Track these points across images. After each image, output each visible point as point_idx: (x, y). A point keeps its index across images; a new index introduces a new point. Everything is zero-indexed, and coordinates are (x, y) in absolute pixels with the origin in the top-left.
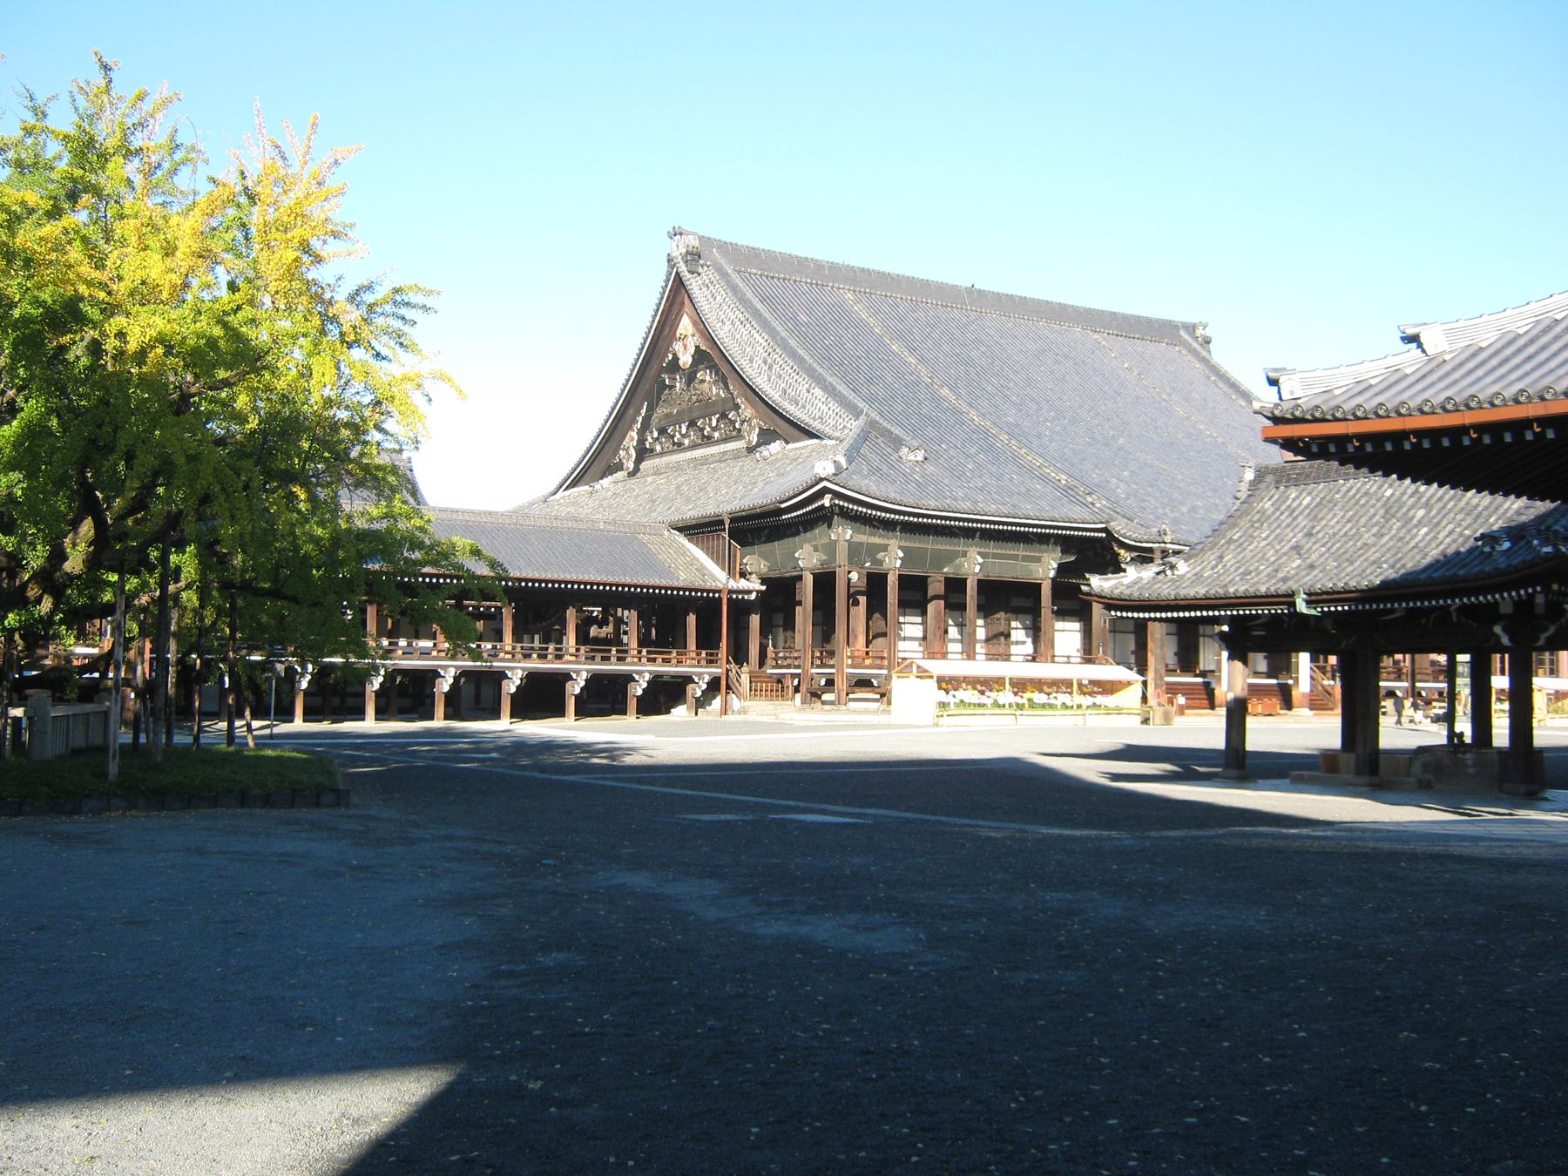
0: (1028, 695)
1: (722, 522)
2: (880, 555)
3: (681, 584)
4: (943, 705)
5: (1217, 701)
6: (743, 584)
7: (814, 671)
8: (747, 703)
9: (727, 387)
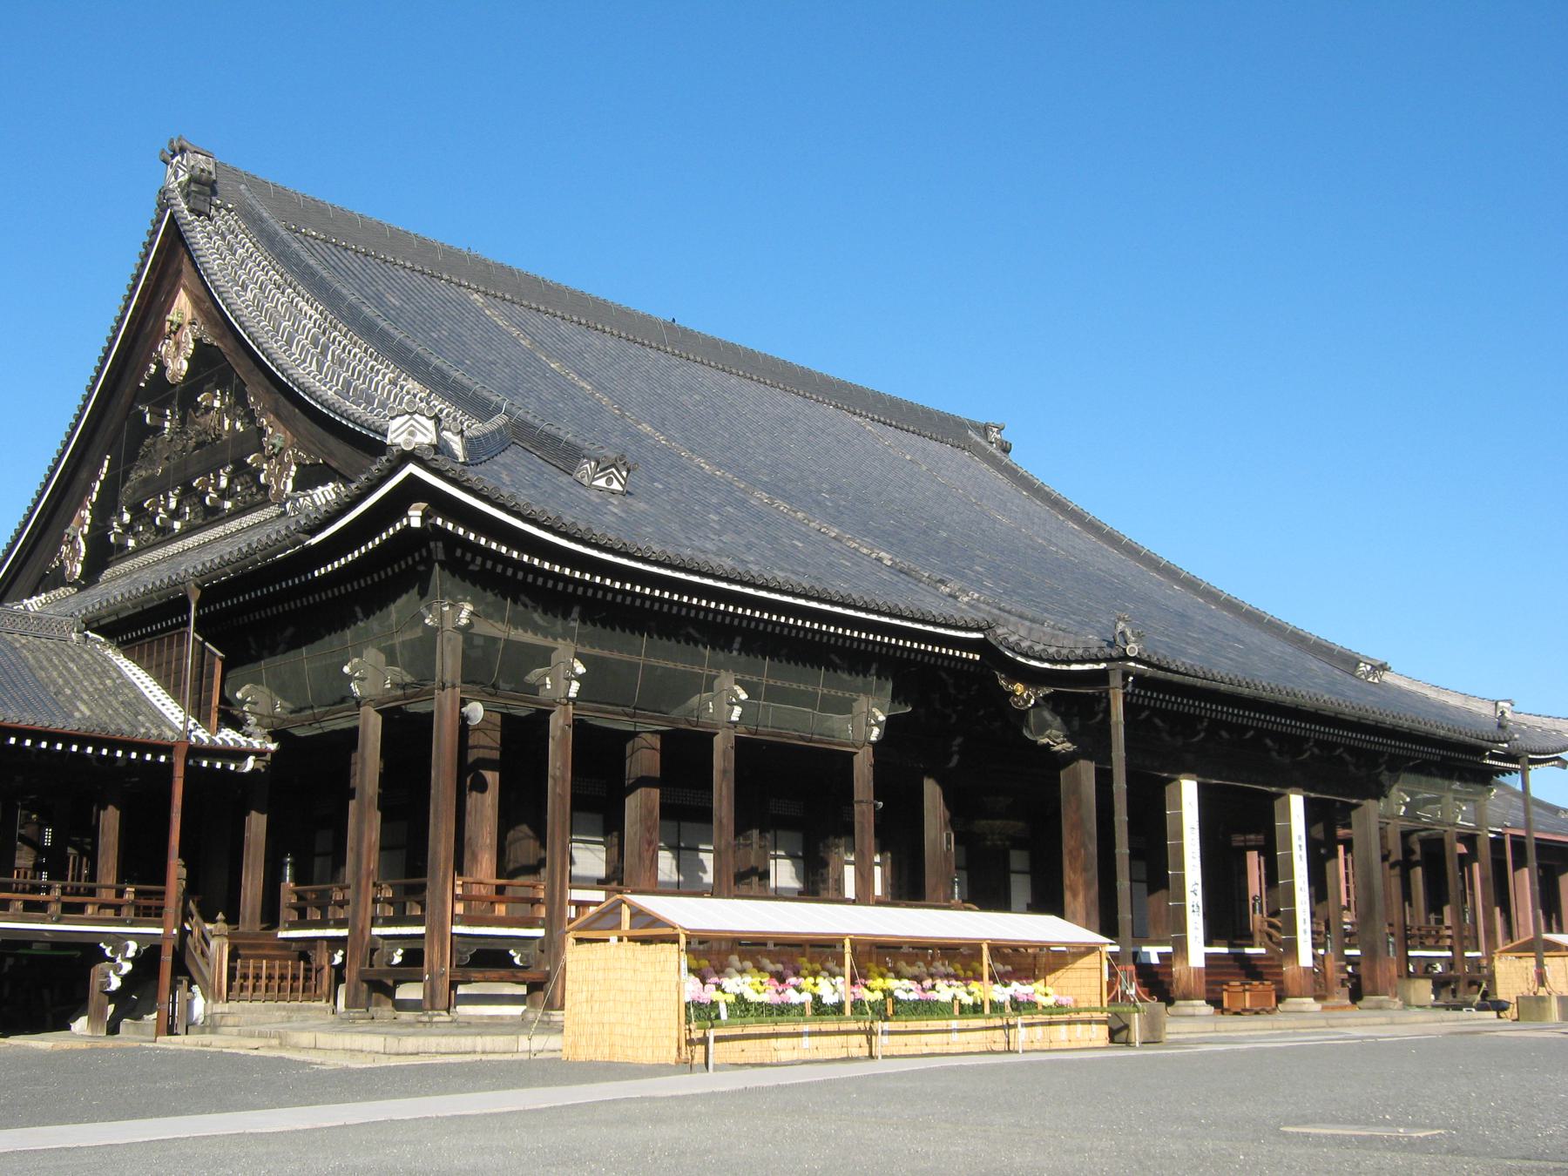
0: (878, 983)
1: (181, 605)
2: (532, 676)
3: (72, 726)
4: (702, 1012)
5: (1177, 990)
6: (228, 736)
7: (376, 931)
8: (221, 1007)
9: (250, 417)
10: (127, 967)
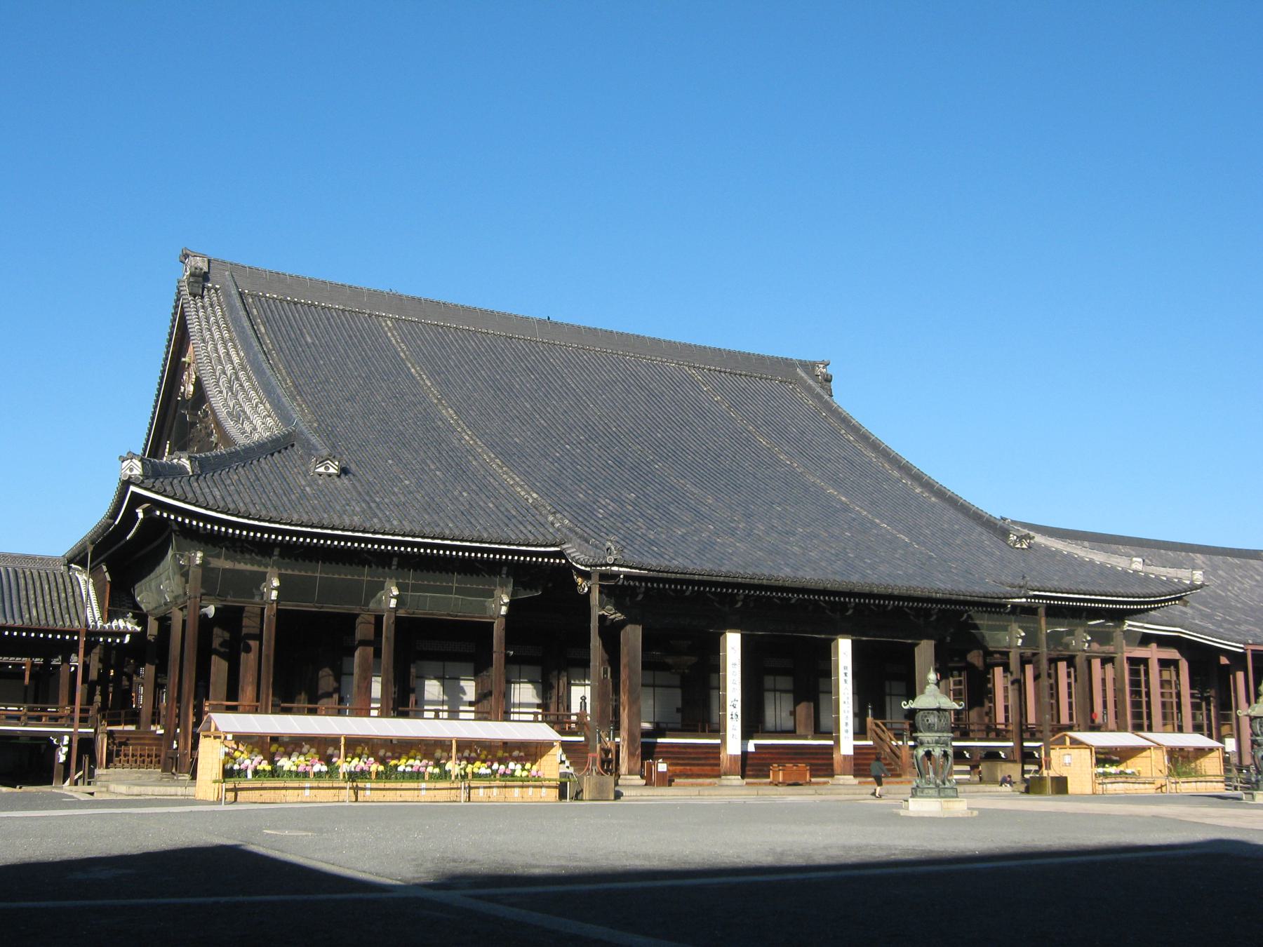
6: (119, 624)
8: (104, 771)
10: (65, 749)
